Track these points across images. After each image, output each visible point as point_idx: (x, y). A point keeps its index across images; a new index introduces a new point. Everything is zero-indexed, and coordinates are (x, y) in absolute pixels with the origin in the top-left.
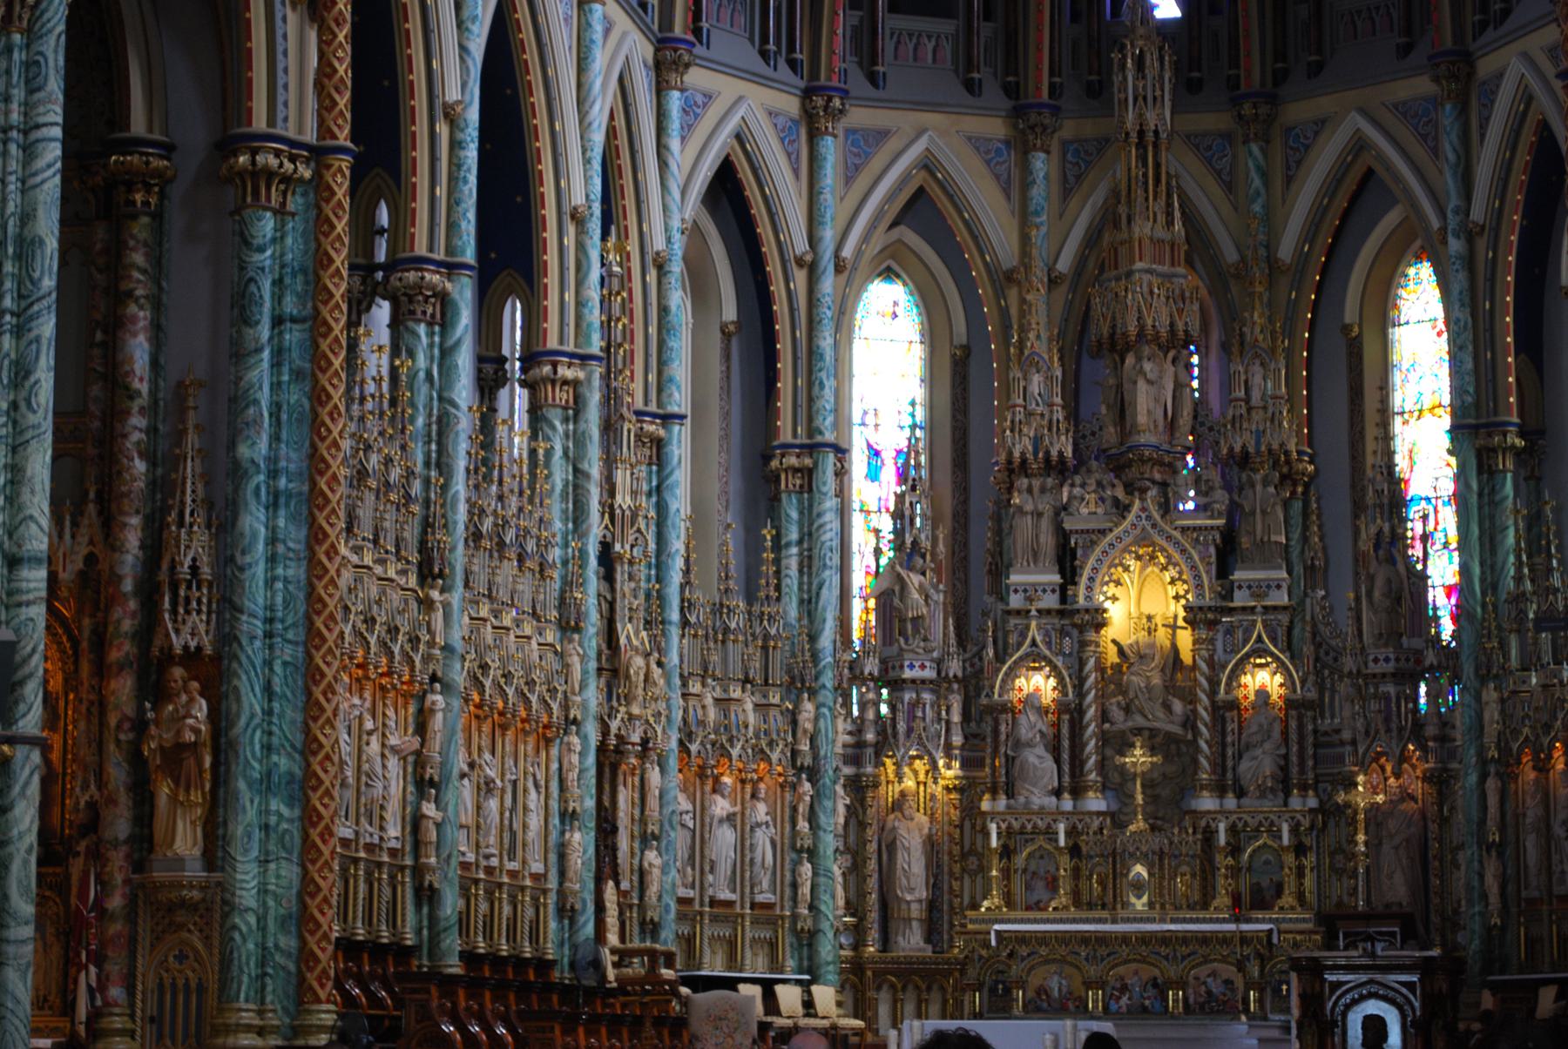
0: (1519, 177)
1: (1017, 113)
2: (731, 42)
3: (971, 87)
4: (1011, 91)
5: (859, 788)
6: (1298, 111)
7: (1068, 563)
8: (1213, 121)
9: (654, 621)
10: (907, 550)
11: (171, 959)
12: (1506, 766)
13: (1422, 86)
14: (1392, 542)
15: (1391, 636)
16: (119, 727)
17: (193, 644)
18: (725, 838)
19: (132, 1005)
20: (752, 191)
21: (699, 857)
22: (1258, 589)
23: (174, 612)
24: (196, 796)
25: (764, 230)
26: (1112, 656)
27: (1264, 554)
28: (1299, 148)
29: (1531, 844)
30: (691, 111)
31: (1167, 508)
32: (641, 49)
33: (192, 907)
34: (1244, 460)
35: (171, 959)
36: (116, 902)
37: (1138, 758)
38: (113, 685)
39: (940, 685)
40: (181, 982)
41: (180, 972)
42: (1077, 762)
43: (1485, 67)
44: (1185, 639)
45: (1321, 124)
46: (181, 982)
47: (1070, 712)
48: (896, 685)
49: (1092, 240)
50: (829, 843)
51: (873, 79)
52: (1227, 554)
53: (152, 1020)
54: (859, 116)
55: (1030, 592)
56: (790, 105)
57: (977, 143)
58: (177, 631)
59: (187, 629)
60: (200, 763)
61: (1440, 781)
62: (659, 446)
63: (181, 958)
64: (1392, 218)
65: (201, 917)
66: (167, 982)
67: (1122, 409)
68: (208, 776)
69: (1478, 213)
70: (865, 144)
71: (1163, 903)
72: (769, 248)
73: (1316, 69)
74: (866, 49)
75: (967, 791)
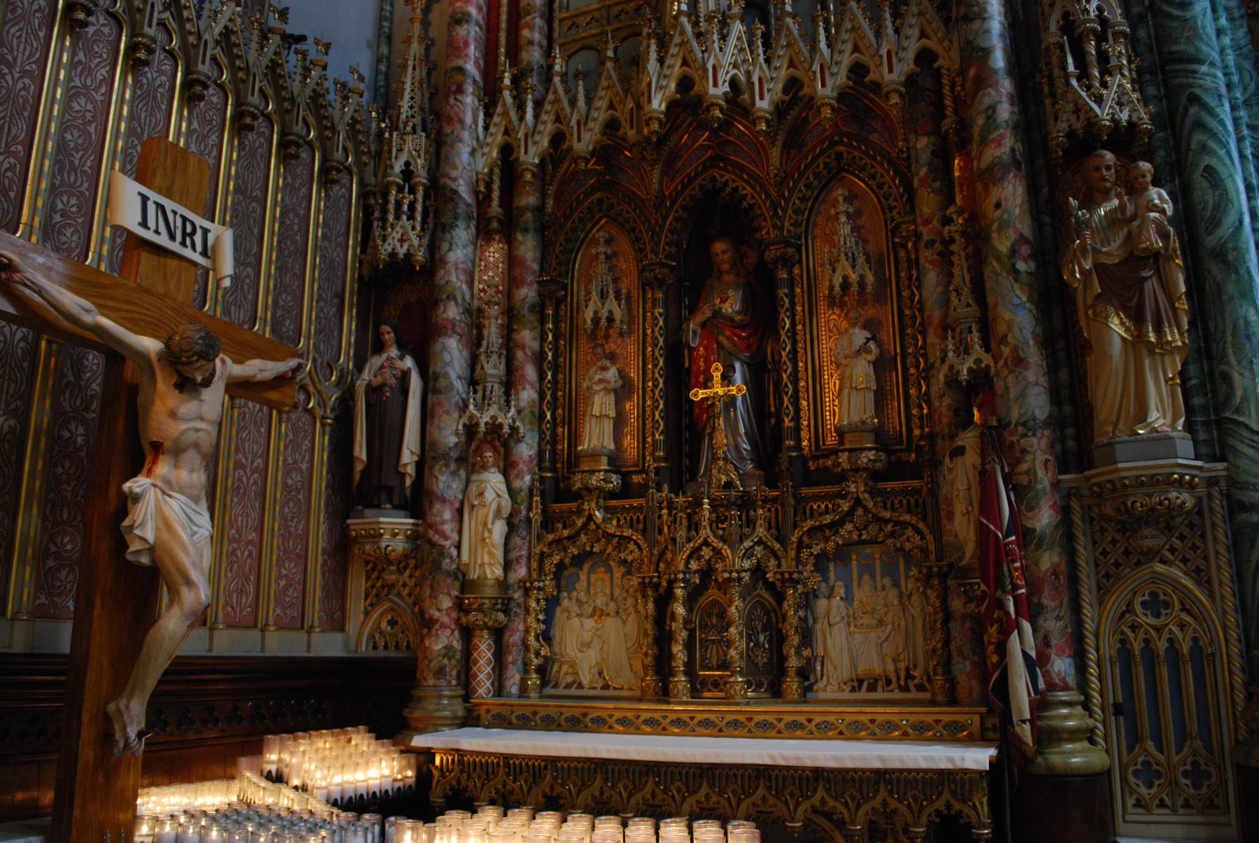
11: (1139, 609)
16: (1013, 251)
17: (1124, 116)
19: (1083, 685)
23: (1083, 75)
24: (1174, 337)
33: (1165, 519)
35: (1139, 609)
36: (1044, 518)
38: (995, 194)
40: (1162, 646)
41: (1158, 630)
46: (1162, 646)
53: (1118, 709)
58: (1099, 100)
59: (1110, 95)
60: (1167, 286)
63: (1156, 605)
65: (1182, 538)
66: (1137, 646)
68: (1183, 305)
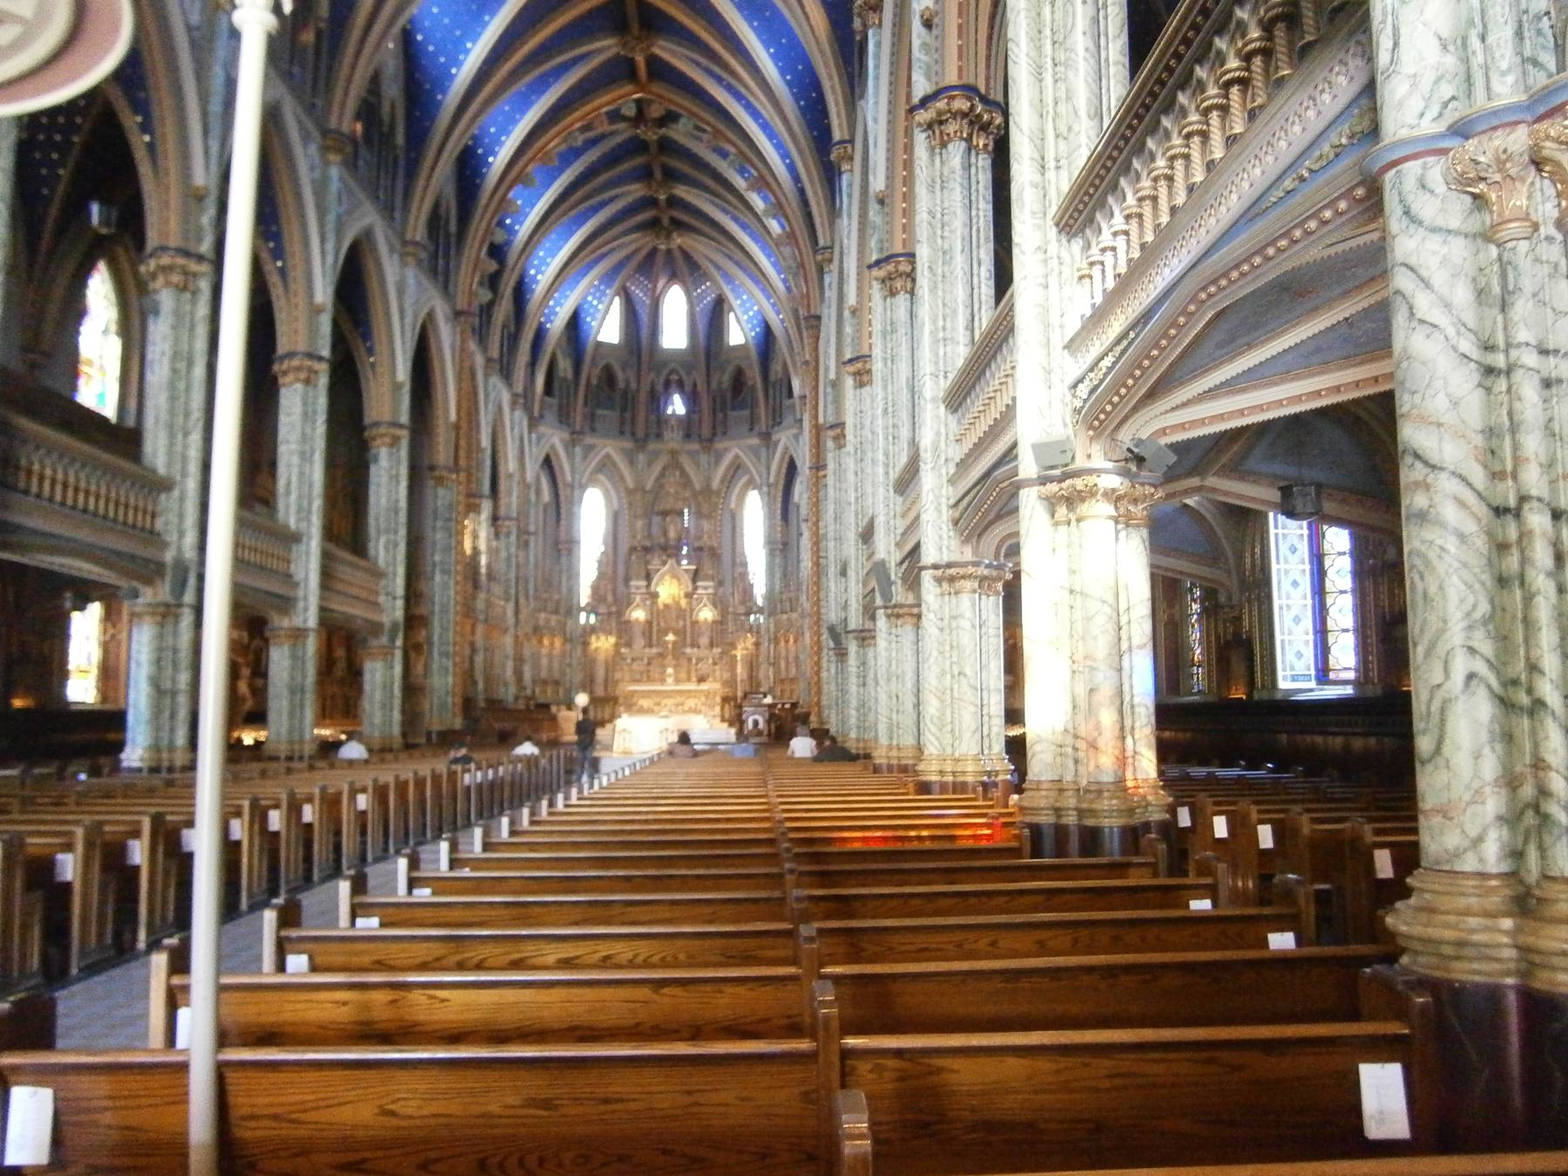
0: (784, 471)
1: (636, 441)
2: (551, 416)
3: (622, 433)
4: (633, 434)
5: (586, 644)
6: (719, 445)
7: (648, 577)
8: (695, 446)
9: (527, 598)
10: (601, 576)
12: (776, 641)
13: (755, 441)
14: (744, 575)
15: (743, 602)
18: (544, 662)
20: (554, 463)
21: (536, 666)
22: (706, 588)
25: (558, 474)
26: (661, 606)
27: (706, 578)
28: (719, 458)
29: (783, 664)
30: (539, 439)
31: (679, 564)
32: (525, 423)
34: (700, 549)
37: (670, 637)
39: (609, 614)
42: (650, 638)
43: (775, 437)
44: (683, 603)
45: (726, 450)
47: (649, 623)
48: (597, 614)
49: (658, 480)
50: (575, 662)
51: (593, 430)
52: (695, 577)
54: (589, 440)
55: (638, 588)
56: (566, 436)
57: (623, 450)
61: (757, 644)
62: (527, 544)
64: (745, 479)
67: (665, 533)
69: (772, 480)
70: (589, 449)
71: (677, 681)
72: (559, 480)
73: (725, 433)
74: (591, 418)
75: (617, 645)
